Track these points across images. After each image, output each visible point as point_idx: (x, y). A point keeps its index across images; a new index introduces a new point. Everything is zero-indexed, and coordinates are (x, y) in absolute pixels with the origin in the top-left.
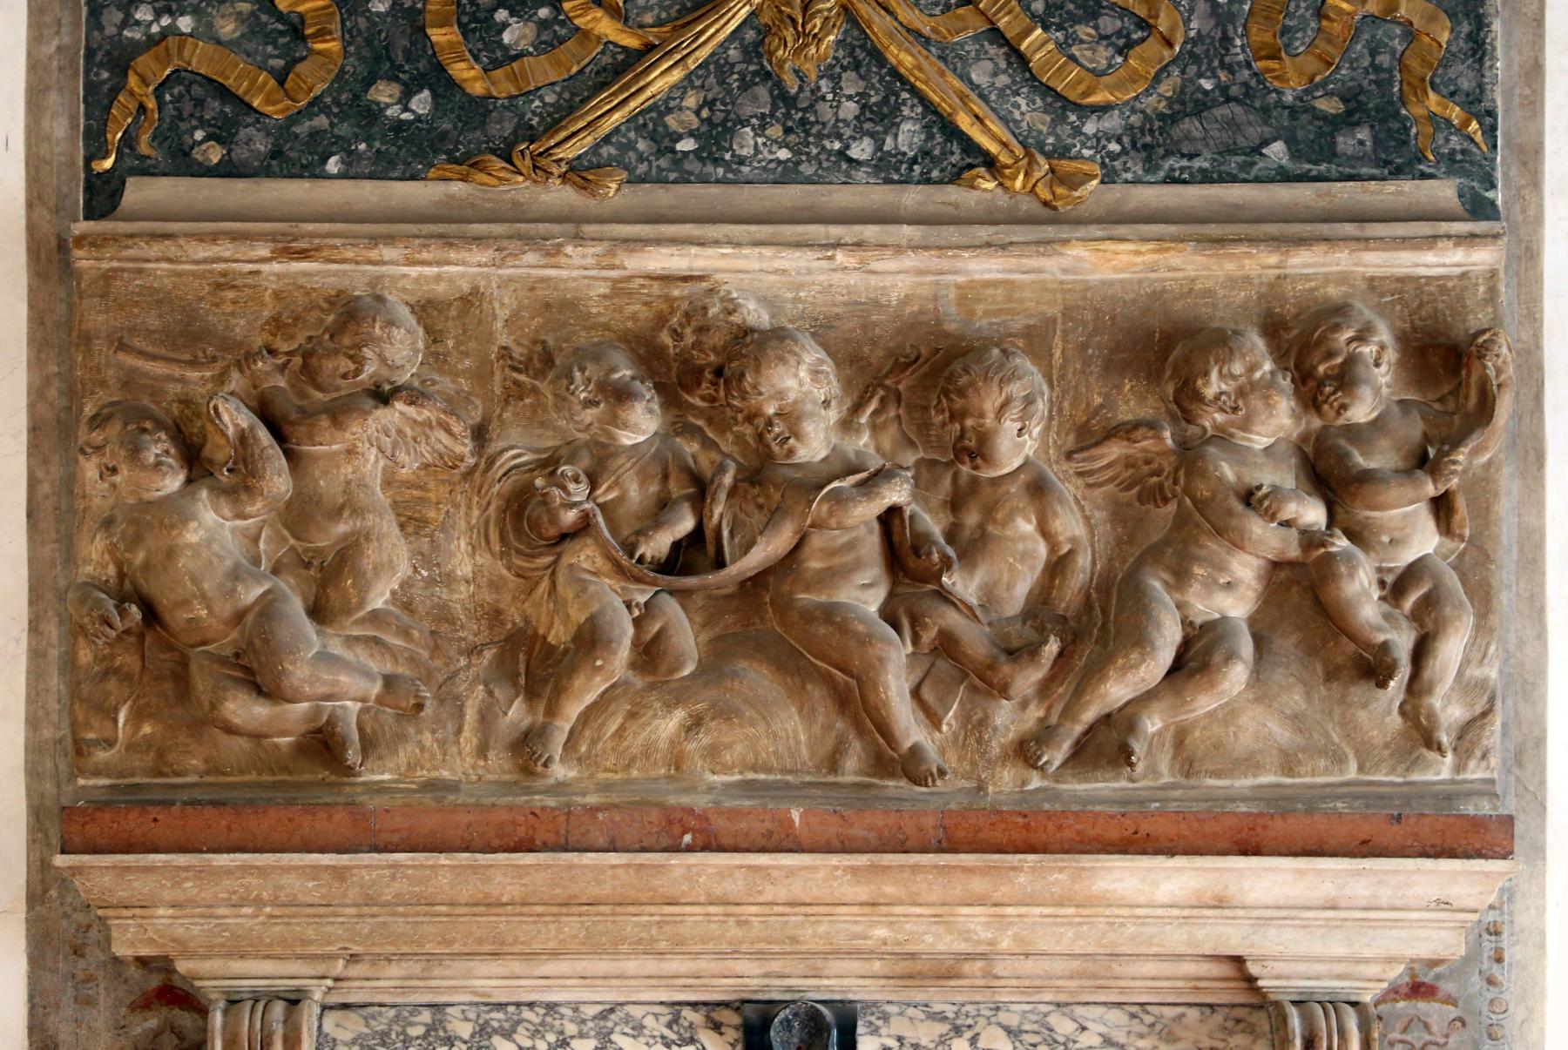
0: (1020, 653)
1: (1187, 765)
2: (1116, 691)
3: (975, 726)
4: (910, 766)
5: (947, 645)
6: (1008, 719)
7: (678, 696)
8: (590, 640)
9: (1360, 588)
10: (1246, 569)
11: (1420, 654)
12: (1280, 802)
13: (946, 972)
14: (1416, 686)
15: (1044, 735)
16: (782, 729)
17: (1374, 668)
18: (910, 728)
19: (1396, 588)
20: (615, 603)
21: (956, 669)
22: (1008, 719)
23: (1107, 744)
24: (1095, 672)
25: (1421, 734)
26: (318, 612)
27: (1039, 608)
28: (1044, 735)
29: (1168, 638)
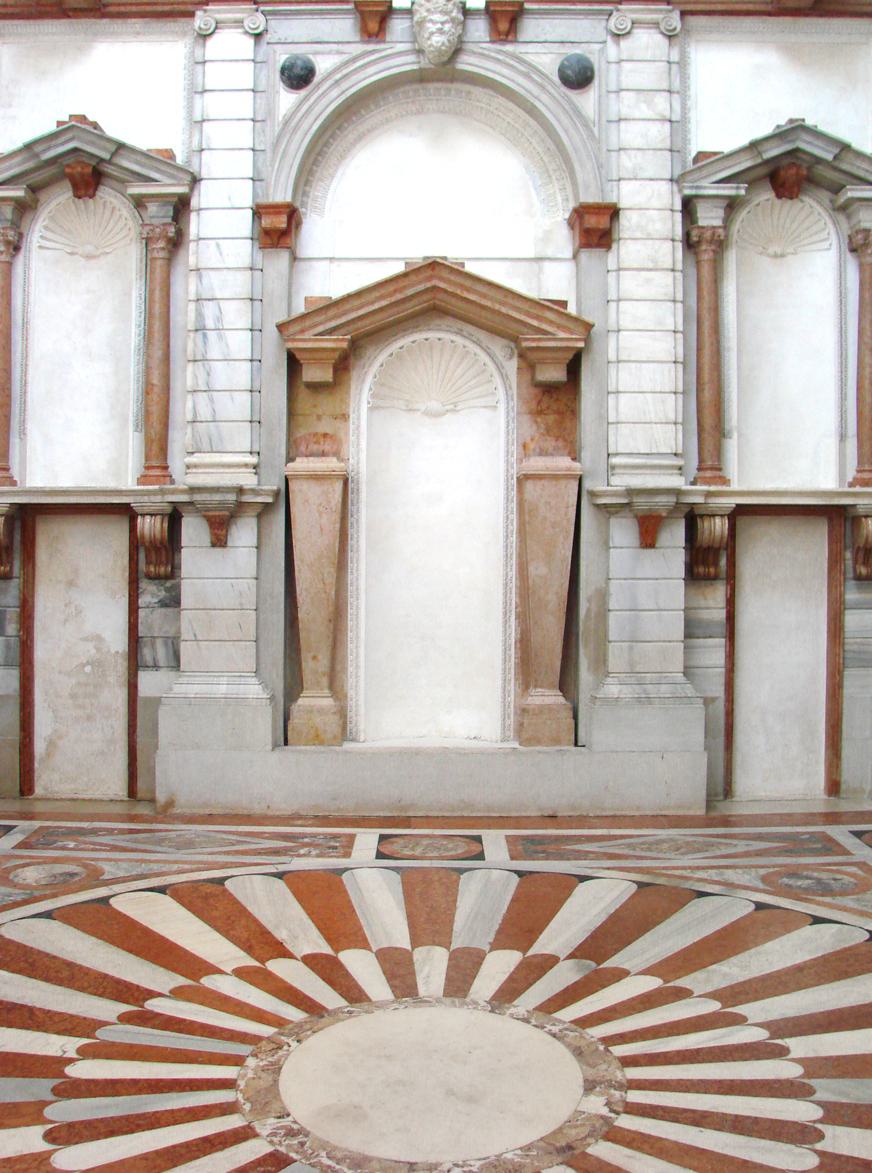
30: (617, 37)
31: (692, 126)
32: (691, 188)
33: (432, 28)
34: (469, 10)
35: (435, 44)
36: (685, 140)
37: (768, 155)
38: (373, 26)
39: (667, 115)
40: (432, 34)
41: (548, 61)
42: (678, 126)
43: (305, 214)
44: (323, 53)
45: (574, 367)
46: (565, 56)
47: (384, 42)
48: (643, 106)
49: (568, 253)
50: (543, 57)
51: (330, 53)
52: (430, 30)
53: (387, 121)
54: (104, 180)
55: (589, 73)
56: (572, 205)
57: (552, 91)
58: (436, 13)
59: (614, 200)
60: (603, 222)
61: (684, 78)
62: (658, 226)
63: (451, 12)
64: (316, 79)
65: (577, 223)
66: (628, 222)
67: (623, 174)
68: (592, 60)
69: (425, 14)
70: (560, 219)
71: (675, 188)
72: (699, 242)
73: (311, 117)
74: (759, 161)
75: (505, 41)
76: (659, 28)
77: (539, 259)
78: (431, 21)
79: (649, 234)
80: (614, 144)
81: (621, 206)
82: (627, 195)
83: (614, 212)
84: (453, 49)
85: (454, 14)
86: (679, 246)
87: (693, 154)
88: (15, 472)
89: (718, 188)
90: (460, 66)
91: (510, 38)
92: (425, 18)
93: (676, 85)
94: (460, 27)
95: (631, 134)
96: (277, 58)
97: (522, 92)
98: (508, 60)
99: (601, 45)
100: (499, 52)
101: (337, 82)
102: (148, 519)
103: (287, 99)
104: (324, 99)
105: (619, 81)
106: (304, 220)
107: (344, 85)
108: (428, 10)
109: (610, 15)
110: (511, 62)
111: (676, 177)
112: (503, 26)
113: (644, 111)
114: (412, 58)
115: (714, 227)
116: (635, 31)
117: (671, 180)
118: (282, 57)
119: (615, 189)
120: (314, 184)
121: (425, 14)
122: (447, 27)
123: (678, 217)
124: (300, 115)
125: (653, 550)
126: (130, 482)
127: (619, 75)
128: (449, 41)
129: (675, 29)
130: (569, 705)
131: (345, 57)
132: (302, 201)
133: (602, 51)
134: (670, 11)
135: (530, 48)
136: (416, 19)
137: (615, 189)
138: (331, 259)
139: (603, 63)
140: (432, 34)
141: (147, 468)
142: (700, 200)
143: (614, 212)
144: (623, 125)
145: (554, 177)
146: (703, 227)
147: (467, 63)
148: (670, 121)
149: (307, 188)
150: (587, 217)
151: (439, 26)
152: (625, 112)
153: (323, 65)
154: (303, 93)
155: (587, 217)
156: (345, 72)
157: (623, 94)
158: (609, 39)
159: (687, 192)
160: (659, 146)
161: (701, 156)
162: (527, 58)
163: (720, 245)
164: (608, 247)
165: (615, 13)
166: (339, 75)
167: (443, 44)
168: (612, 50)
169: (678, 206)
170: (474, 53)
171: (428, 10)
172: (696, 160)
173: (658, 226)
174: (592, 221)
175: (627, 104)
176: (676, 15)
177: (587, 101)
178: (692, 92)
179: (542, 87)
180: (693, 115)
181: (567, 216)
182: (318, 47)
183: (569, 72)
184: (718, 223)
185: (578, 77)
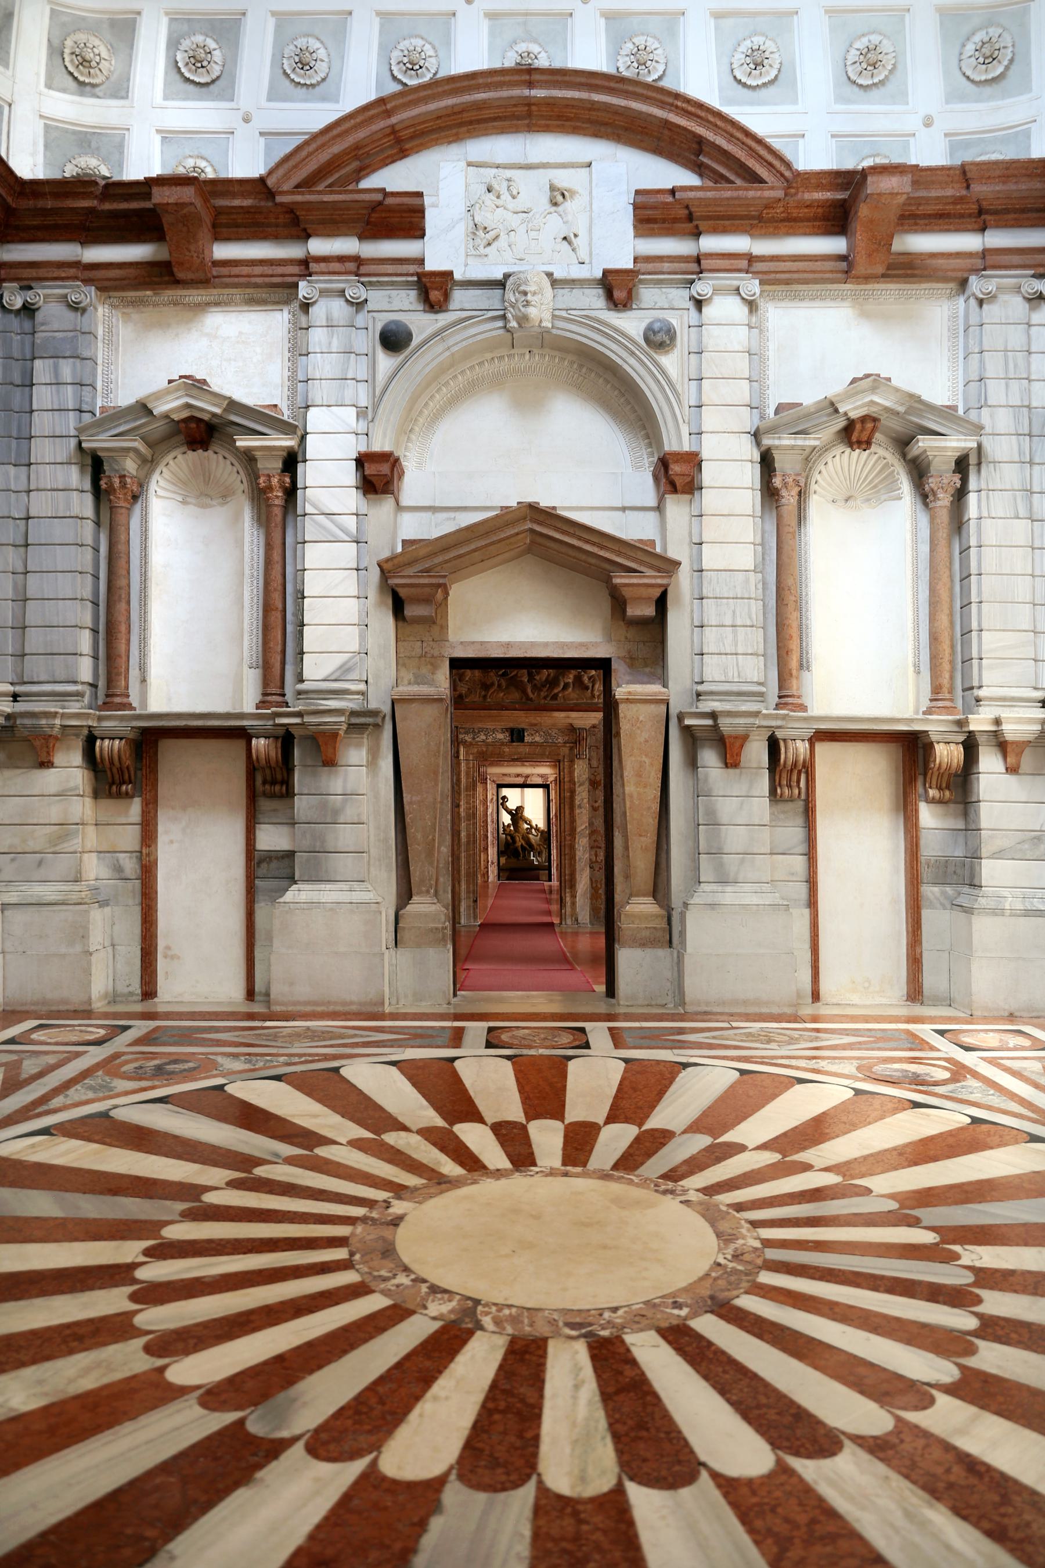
0: (544, 686)
1: (565, 700)
2: (556, 691)
3: (539, 695)
4: (531, 700)
5: (535, 685)
6: (543, 694)
7: (503, 691)
8: (493, 684)
9: (586, 679)
10: (571, 676)
11: (593, 686)
12: (576, 705)
13: (536, 725)
14: (593, 690)
15: (547, 696)
16: (516, 695)
17: (587, 688)
18: (531, 695)
19: (590, 678)
20: (495, 680)
21: (535, 688)
22: (543, 694)
23: (555, 697)
24: (553, 689)
25: (593, 696)
26: (460, 680)
27: (547, 679)
28: (547, 696)
29: (562, 684)
42: (757, 380)
45: (661, 603)
49: (651, 501)
54: (216, 435)
56: (656, 459)
64: (415, 342)
81: (705, 455)
83: (694, 460)
88: (134, 699)
89: (795, 439)
102: (262, 741)
103: (385, 362)
116: (715, 297)
118: (381, 321)
125: (737, 771)
126: (249, 706)
130: (664, 913)
141: (265, 694)
154: (402, 357)
169: (757, 457)
172: (776, 413)
177: (669, 361)
185: (659, 339)
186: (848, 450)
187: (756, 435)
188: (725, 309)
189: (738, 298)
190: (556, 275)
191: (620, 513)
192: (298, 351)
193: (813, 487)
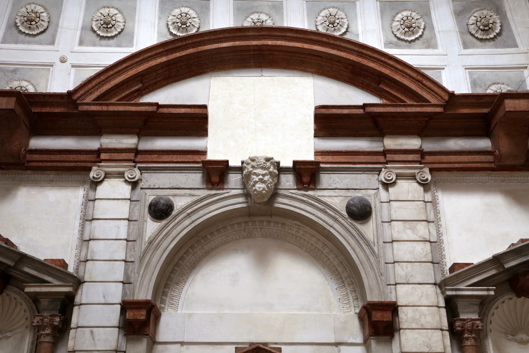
30: (387, 185)
31: (445, 245)
32: (452, 290)
33: (256, 179)
34: (282, 168)
35: (258, 189)
36: (442, 256)
37: (507, 266)
38: (215, 179)
39: (427, 237)
40: (256, 182)
41: (339, 202)
43: (163, 308)
44: (180, 195)
46: (350, 198)
47: (223, 189)
48: (409, 232)
50: (335, 198)
51: (184, 195)
52: (254, 180)
53: (226, 243)
55: (368, 209)
56: (361, 305)
57: (343, 222)
58: (259, 168)
59: (394, 300)
60: (387, 316)
61: (436, 212)
62: (429, 319)
63: (269, 168)
65: (366, 317)
66: (405, 316)
67: (398, 281)
68: (370, 201)
69: (251, 169)
70: (352, 313)
71: (439, 291)
72: (462, 332)
73: (169, 239)
74: (502, 270)
75: (307, 189)
76: (415, 179)
77: (337, 344)
78: (255, 174)
79: (422, 325)
80: (390, 259)
82: (403, 295)
84: (271, 193)
85: (271, 170)
86: (447, 333)
87: (449, 265)
90: (277, 205)
91: (311, 186)
92: (251, 171)
93: (432, 217)
94: (275, 179)
95: (402, 251)
96: (147, 198)
97: (321, 222)
98: (310, 201)
99: (375, 191)
100: (304, 195)
101: (189, 215)
104: (180, 228)
105: (390, 215)
106: (162, 313)
107: (194, 217)
108: (253, 167)
109: (380, 171)
110: (313, 202)
111: (438, 282)
112: (306, 179)
113: (409, 235)
114: (241, 199)
115: (472, 320)
116: (398, 181)
117: (435, 284)
119: (393, 291)
120: (171, 287)
121: (251, 169)
122: (266, 178)
123: (443, 311)
124: (161, 237)
127: (390, 210)
128: (268, 187)
129: (427, 180)
131: (195, 199)
132: (162, 299)
133: (376, 195)
134: (421, 168)
135: (325, 193)
136: (244, 172)
137: (393, 291)
138: (182, 343)
139: (378, 202)
140: (256, 182)
142: (459, 300)
143: (393, 308)
144: (395, 244)
145: (346, 283)
146: (464, 320)
147: (282, 203)
148: (429, 241)
149: (167, 290)
150: (374, 313)
151: (261, 177)
152: (396, 236)
153: (179, 203)
154: (164, 222)
155: (374, 313)
156: (194, 208)
157: (393, 223)
158: (381, 187)
159: (449, 293)
160: (423, 260)
161: (454, 267)
162: (322, 199)
163: (480, 335)
164: (392, 336)
165: (383, 170)
166: (189, 211)
167: (264, 189)
168: (383, 194)
169: (442, 303)
170: (286, 197)
171: (253, 167)
173: (429, 319)
174: (377, 316)
175: (398, 230)
176: (427, 170)
178: (442, 222)
179: (336, 220)
180: (444, 238)
181: (358, 311)
182: (177, 192)
183: (354, 208)
184: (475, 316)
185: (360, 212)
186: (515, 298)
187: (442, 285)
188: (407, 188)
189: (415, 181)
190: (282, 165)
191: (334, 347)
192: (87, 219)
193: (490, 327)
